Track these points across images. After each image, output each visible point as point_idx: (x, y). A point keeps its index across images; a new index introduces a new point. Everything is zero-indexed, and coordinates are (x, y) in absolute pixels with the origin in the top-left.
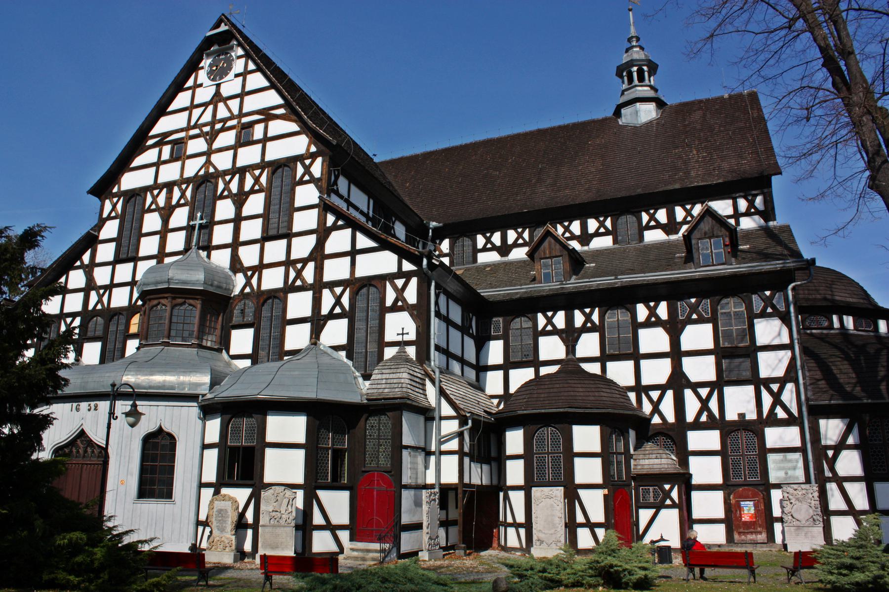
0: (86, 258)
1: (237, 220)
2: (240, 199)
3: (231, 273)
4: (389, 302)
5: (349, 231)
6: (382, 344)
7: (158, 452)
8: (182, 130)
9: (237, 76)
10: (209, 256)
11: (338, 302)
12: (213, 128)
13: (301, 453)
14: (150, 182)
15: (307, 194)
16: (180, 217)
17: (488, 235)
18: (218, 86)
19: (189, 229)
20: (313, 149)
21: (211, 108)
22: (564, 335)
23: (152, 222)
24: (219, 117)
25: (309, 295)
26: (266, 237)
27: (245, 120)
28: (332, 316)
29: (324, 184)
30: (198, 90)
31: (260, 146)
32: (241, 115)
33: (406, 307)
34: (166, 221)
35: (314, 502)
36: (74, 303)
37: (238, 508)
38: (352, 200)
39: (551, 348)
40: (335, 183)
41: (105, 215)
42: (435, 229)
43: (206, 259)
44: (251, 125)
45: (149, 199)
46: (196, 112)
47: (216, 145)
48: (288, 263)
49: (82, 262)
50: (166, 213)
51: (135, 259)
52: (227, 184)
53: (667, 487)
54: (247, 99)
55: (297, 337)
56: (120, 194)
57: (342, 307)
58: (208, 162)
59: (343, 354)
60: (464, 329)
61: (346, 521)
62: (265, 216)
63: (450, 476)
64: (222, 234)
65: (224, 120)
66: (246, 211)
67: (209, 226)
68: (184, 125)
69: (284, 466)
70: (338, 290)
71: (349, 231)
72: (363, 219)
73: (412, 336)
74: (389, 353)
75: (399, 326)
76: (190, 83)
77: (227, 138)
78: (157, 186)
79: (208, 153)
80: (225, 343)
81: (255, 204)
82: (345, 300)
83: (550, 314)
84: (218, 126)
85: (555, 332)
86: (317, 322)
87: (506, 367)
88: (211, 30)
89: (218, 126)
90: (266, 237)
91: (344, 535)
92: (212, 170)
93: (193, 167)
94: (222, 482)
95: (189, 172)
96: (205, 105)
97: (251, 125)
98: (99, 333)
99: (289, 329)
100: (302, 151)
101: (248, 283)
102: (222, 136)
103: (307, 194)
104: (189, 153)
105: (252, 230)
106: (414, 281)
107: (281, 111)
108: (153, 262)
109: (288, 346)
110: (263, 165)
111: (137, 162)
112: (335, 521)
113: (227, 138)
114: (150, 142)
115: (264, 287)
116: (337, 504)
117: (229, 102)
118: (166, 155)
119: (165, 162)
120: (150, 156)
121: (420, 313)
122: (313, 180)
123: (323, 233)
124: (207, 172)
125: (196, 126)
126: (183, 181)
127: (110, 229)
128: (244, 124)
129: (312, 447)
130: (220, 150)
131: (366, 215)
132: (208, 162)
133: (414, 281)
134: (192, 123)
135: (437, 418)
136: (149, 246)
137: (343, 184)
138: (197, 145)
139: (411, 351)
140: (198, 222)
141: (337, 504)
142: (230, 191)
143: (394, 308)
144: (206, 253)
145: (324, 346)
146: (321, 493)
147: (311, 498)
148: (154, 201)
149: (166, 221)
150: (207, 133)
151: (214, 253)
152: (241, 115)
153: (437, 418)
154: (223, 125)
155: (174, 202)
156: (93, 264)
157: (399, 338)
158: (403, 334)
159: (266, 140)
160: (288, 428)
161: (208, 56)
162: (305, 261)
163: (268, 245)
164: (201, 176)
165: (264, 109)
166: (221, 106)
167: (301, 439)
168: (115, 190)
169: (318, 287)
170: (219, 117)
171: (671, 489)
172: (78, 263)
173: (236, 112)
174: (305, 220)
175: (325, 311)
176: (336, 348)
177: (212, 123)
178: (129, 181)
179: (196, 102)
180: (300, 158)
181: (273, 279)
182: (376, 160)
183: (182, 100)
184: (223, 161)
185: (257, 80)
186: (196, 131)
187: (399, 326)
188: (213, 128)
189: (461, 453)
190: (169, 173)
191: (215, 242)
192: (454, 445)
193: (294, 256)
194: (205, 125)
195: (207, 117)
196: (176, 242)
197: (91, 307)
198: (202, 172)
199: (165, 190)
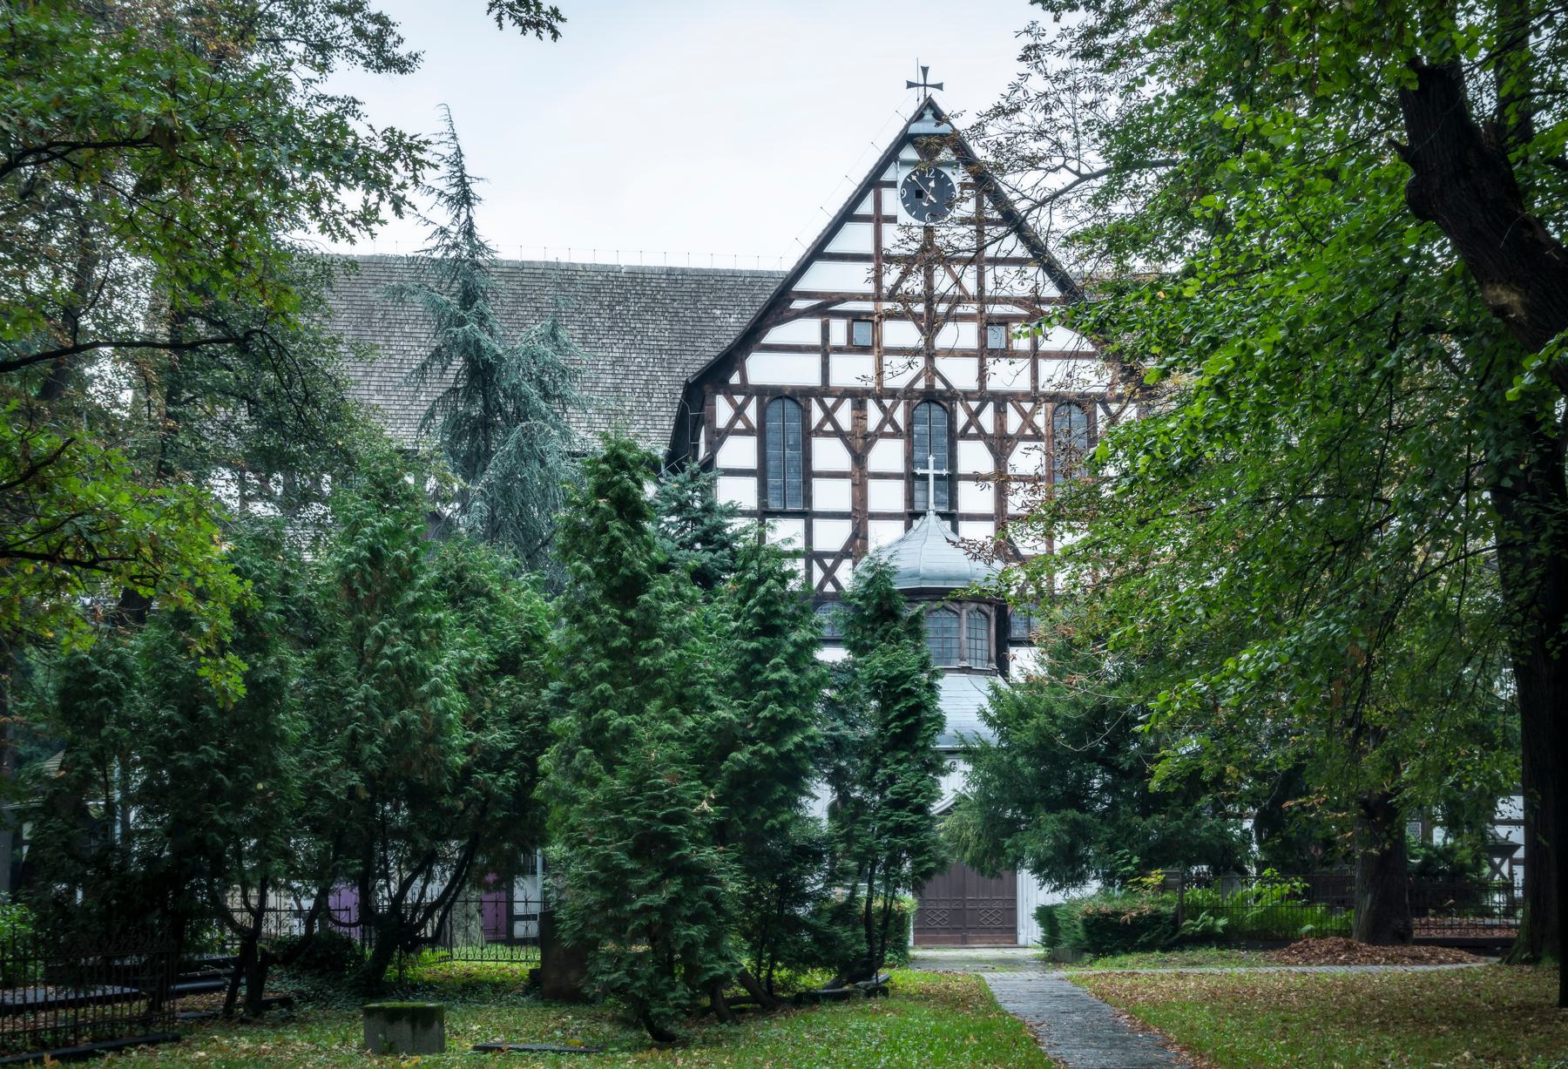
2: (1000, 445)
8: (865, 297)
14: (814, 380)
16: (888, 455)
23: (829, 454)
34: (859, 459)
43: (952, 537)
44: (1004, 321)
45: (817, 414)
50: (859, 444)
52: (974, 416)
53: (1497, 860)
56: (748, 390)
64: (975, 498)
67: (950, 482)
68: (870, 288)
78: (823, 391)
84: (942, 308)
92: (939, 385)
93: (901, 374)
104: (888, 342)
111: (775, 335)
114: (799, 304)
119: (839, 350)
124: (930, 386)
125: (892, 296)
128: (990, 316)
138: (899, 333)
140: (931, 472)
142: (980, 428)
144: (948, 524)
149: (859, 459)
150: (920, 316)
154: (950, 309)
159: (1035, 355)
164: (920, 392)
168: (735, 379)
171: (1502, 863)
178: (762, 369)
183: (856, 238)
188: (929, 308)
190: (850, 371)
199: (847, 404)
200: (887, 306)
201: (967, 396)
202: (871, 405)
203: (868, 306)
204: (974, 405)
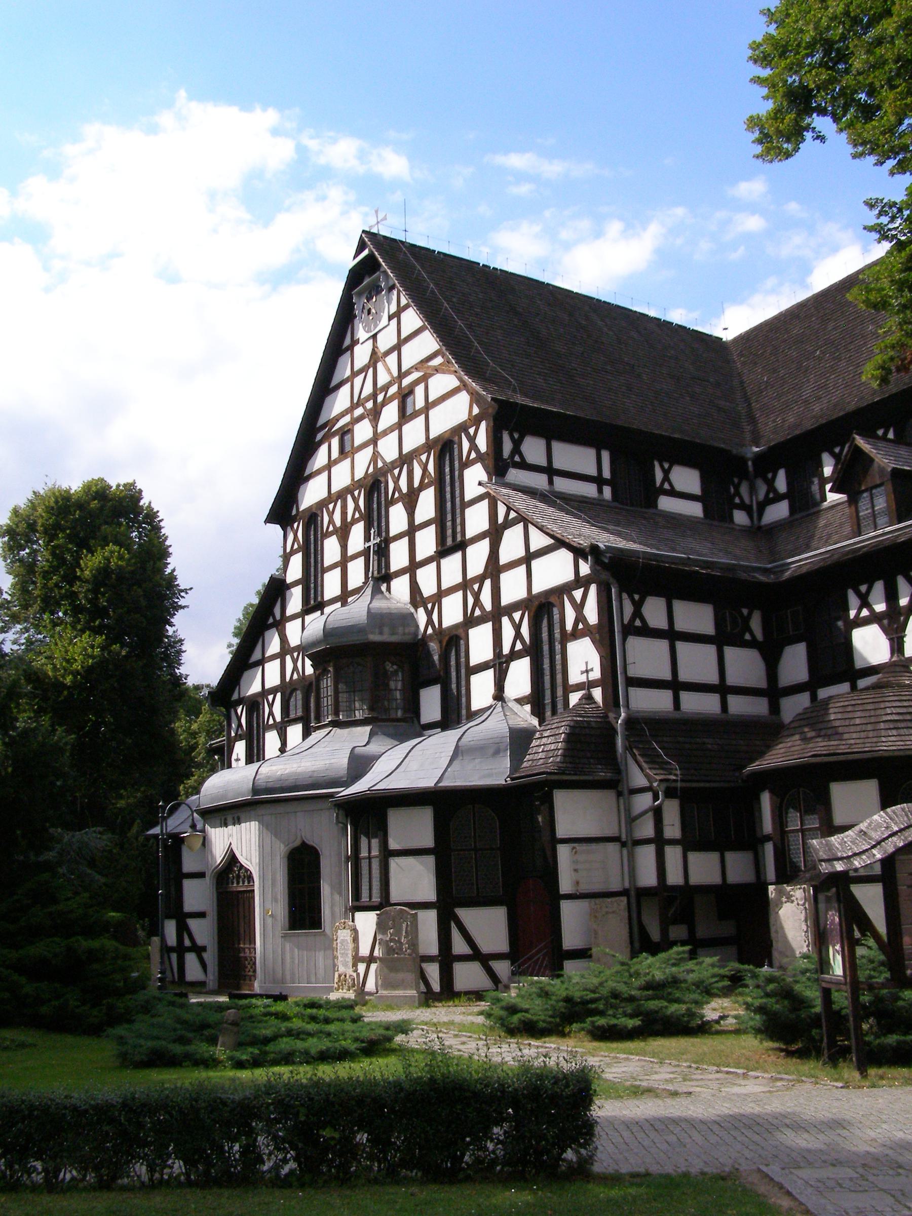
0: (277, 611)
1: (412, 531)
3: (413, 610)
4: (569, 626)
5: (520, 527)
6: (568, 689)
7: (303, 868)
9: (390, 318)
10: (389, 589)
11: (518, 635)
12: (375, 402)
13: (431, 860)
15: (475, 478)
17: (837, 450)
18: (374, 337)
19: (366, 553)
20: (476, 410)
21: (371, 371)
22: (885, 622)
24: (380, 383)
25: (488, 626)
26: (443, 551)
27: (406, 382)
28: (514, 655)
29: (491, 462)
30: (357, 349)
31: (423, 417)
32: (402, 375)
33: (588, 631)
35: (453, 924)
36: (272, 674)
37: (356, 940)
38: (557, 464)
39: (870, 645)
40: (516, 450)
41: (288, 550)
42: (758, 459)
43: (387, 594)
46: (358, 381)
47: (381, 428)
48: (465, 585)
49: (274, 617)
50: (343, 534)
51: (320, 606)
54: (405, 349)
55: (481, 688)
57: (523, 642)
58: (376, 456)
59: (528, 708)
60: (724, 637)
61: (503, 946)
62: (440, 520)
63: (648, 877)
64: (398, 556)
65: (386, 388)
66: (419, 519)
69: (415, 880)
70: (517, 616)
71: (520, 527)
72: (589, 490)
73: (596, 674)
74: (574, 698)
75: (583, 659)
76: (347, 342)
77: (390, 414)
78: (331, 498)
79: (374, 441)
80: (413, 707)
81: (426, 505)
82: (525, 631)
83: (863, 588)
85: (875, 618)
86: (500, 665)
87: (810, 687)
88: (354, 258)
89: (380, 398)
90: (443, 551)
91: (502, 968)
94: (357, 904)
95: (359, 474)
96: (364, 369)
97: (410, 391)
98: (300, 713)
99: (475, 679)
100: (463, 416)
101: (430, 622)
102: (384, 409)
103: (475, 478)
105: (427, 543)
106: (593, 589)
107: (438, 360)
108: (339, 604)
109: (475, 706)
110: (429, 445)
112: (486, 947)
113: (390, 414)
114: (319, 436)
115: (445, 625)
116: (489, 926)
117: (387, 359)
118: (335, 454)
119: (336, 462)
120: (321, 458)
121: (606, 638)
122: (480, 458)
123: (495, 533)
125: (358, 405)
126: (356, 485)
127: (295, 571)
129: (443, 853)
130: (385, 433)
131: (599, 481)
132: (376, 456)
133: (593, 589)
134: (355, 401)
135: (626, 792)
136: (331, 585)
137: (534, 449)
139: (597, 693)
141: (489, 926)
143: (576, 635)
144: (385, 585)
145: (510, 700)
146: (465, 914)
147: (446, 921)
148: (331, 521)
151: (395, 583)
152: (402, 375)
153: (626, 792)
155: (349, 519)
156: (285, 619)
157: (583, 678)
158: (587, 671)
159: (429, 406)
160: (414, 828)
161: (360, 294)
162: (481, 579)
163: (444, 562)
165: (422, 361)
166: (380, 365)
167: (427, 840)
168: (294, 512)
169: (497, 614)
170: (380, 383)
172: (271, 620)
173: (395, 374)
174: (476, 520)
175: (506, 650)
176: (520, 701)
177: (374, 396)
179: (356, 369)
180: (462, 428)
181: (452, 612)
182: (728, 336)
184: (389, 450)
185: (412, 319)
186: (359, 411)
187: (583, 659)
188: (375, 402)
189: (660, 842)
190: (342, 477)
191: (394, 568)
192: (647, 829)
193: (470, 575)
194: (367, 399)
195: (368, 389)
196: (357, 573)
197: (288, 679)
198: (371, 470)
200: (359, 411)
201: (393, 465)
202: (349, 498)
203: (347, 419)
204: (396, 472)
